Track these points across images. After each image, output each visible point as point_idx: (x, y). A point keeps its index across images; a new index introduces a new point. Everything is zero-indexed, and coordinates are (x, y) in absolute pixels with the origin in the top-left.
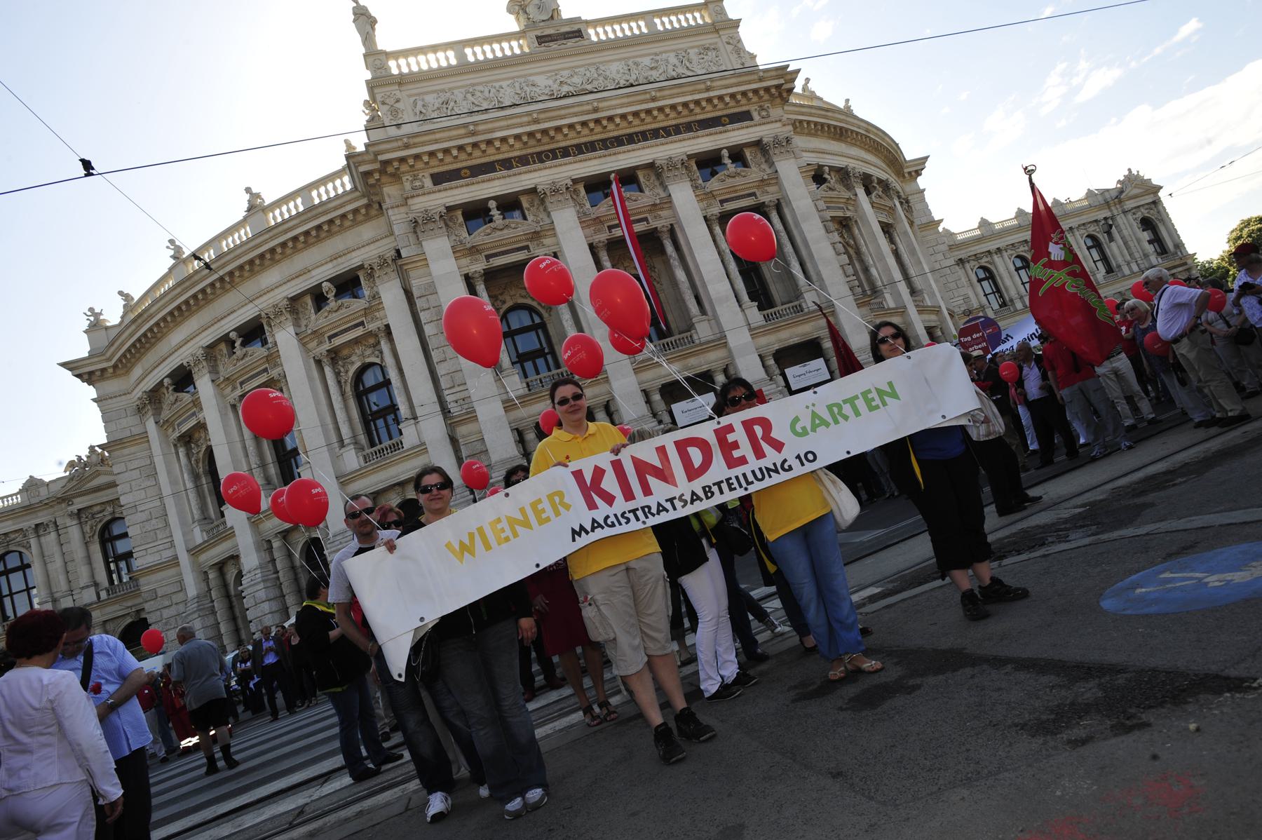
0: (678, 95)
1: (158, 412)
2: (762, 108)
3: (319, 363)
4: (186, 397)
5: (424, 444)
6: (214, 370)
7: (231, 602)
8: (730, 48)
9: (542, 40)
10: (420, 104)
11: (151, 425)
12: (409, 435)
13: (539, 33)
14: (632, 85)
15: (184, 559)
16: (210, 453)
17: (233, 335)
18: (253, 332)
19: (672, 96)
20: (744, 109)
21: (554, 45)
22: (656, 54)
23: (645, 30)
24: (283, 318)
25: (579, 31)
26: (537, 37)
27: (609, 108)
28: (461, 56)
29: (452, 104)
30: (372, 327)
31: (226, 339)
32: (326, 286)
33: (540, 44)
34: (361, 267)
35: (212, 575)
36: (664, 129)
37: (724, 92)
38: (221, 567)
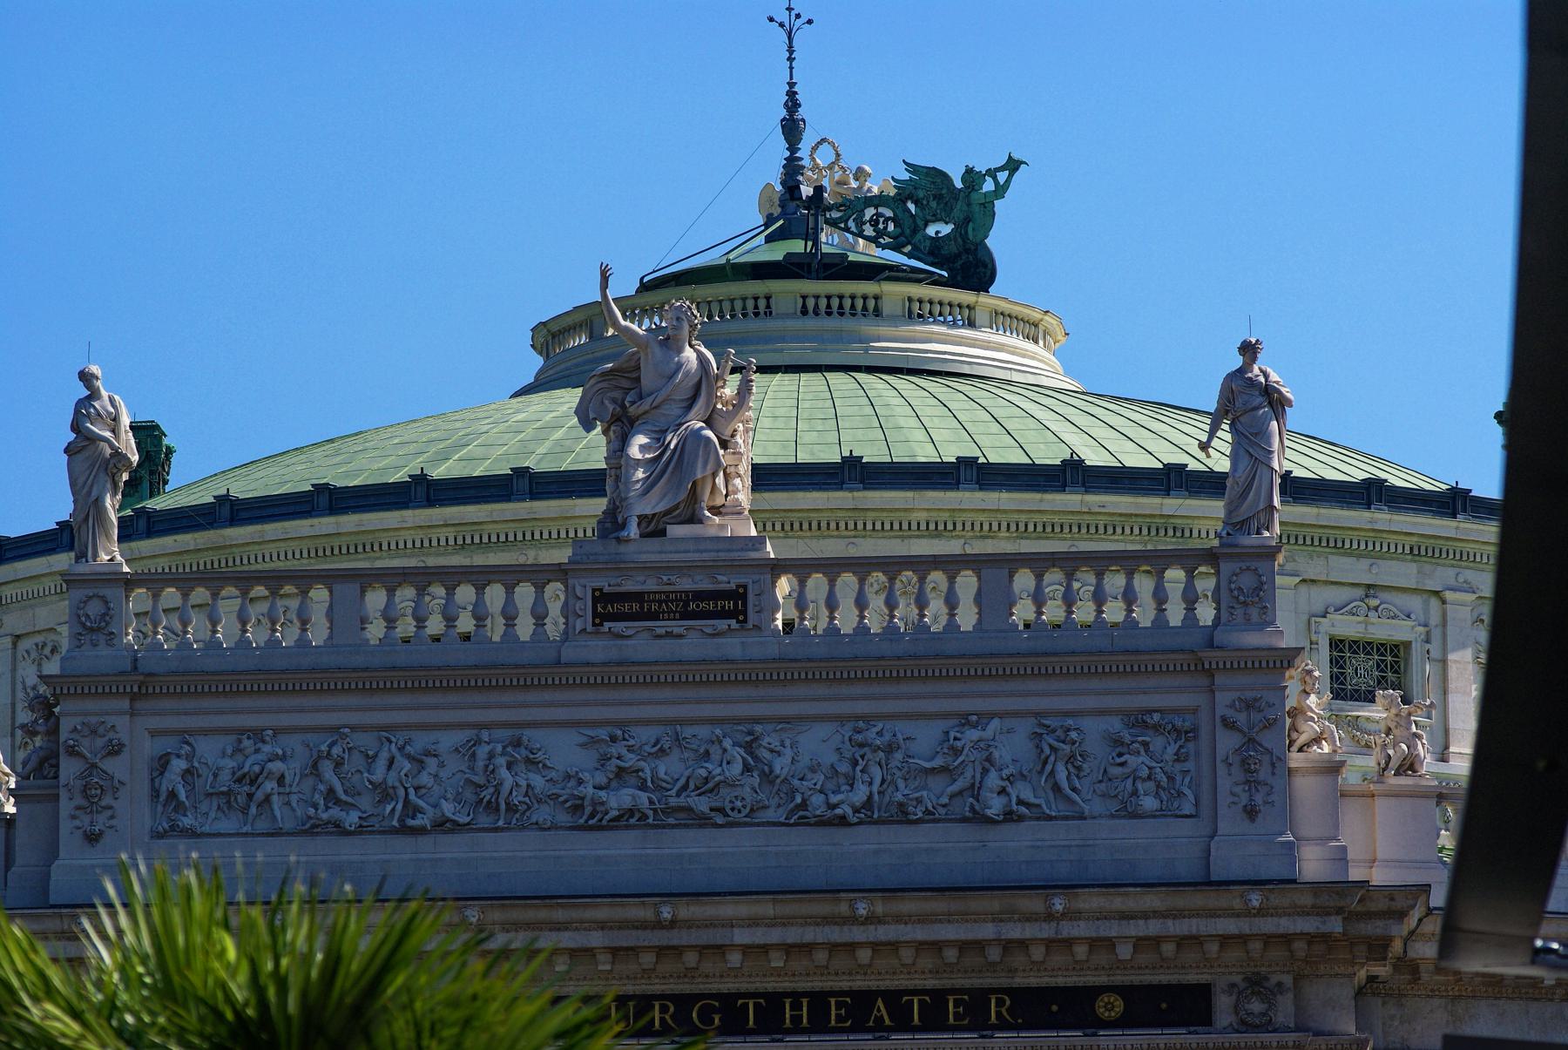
0: (948, 918)
2: (1256, 984)
8: (1227, 742)
9: (611, 607)
10: (179, 765)
13: (605, 583)
14: (843, 821)
19: (924, 919)
20: (1192, 978)
21: (639, 642)
22: (965, 720)
23: (967, 618)
25: (739, 595)
26: (600, 597)
27: (710, 924)
28: (346, 619)
29: (270, 786)
33: (600, 618)
36: (893, 998)
37: (1112, 929)
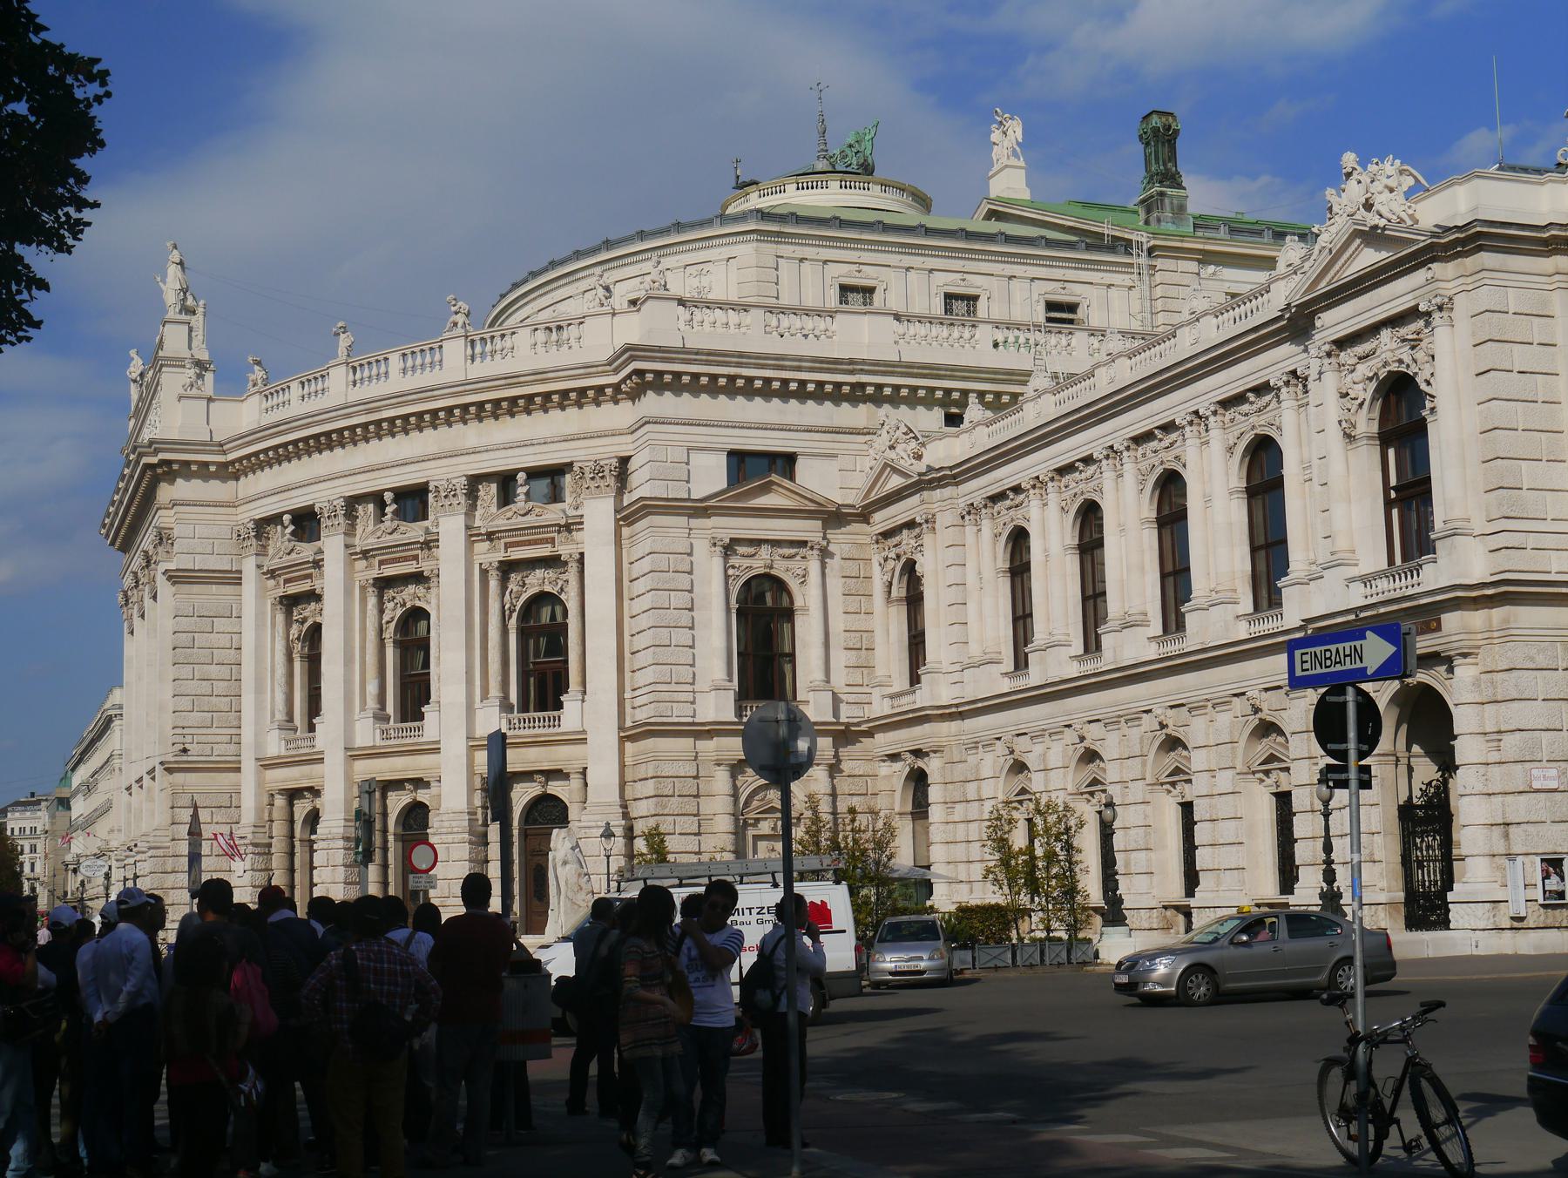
1: (262, 552)
3: (484, 573)
4: (306, 551)
5: (584, 732)
6: (350, 531)
7: (293, 847)
11: (249, 567)
12: (571, 713)
15: (249, 765)
16: (314, 635)
17: (388, 496)
18: (413, 501)
24: (455, 502)
30: (565, 550)
31: (377, 498)
32: (521, 477)
34: (571, 464)
35: (280, 801)
38: (293, 795)
